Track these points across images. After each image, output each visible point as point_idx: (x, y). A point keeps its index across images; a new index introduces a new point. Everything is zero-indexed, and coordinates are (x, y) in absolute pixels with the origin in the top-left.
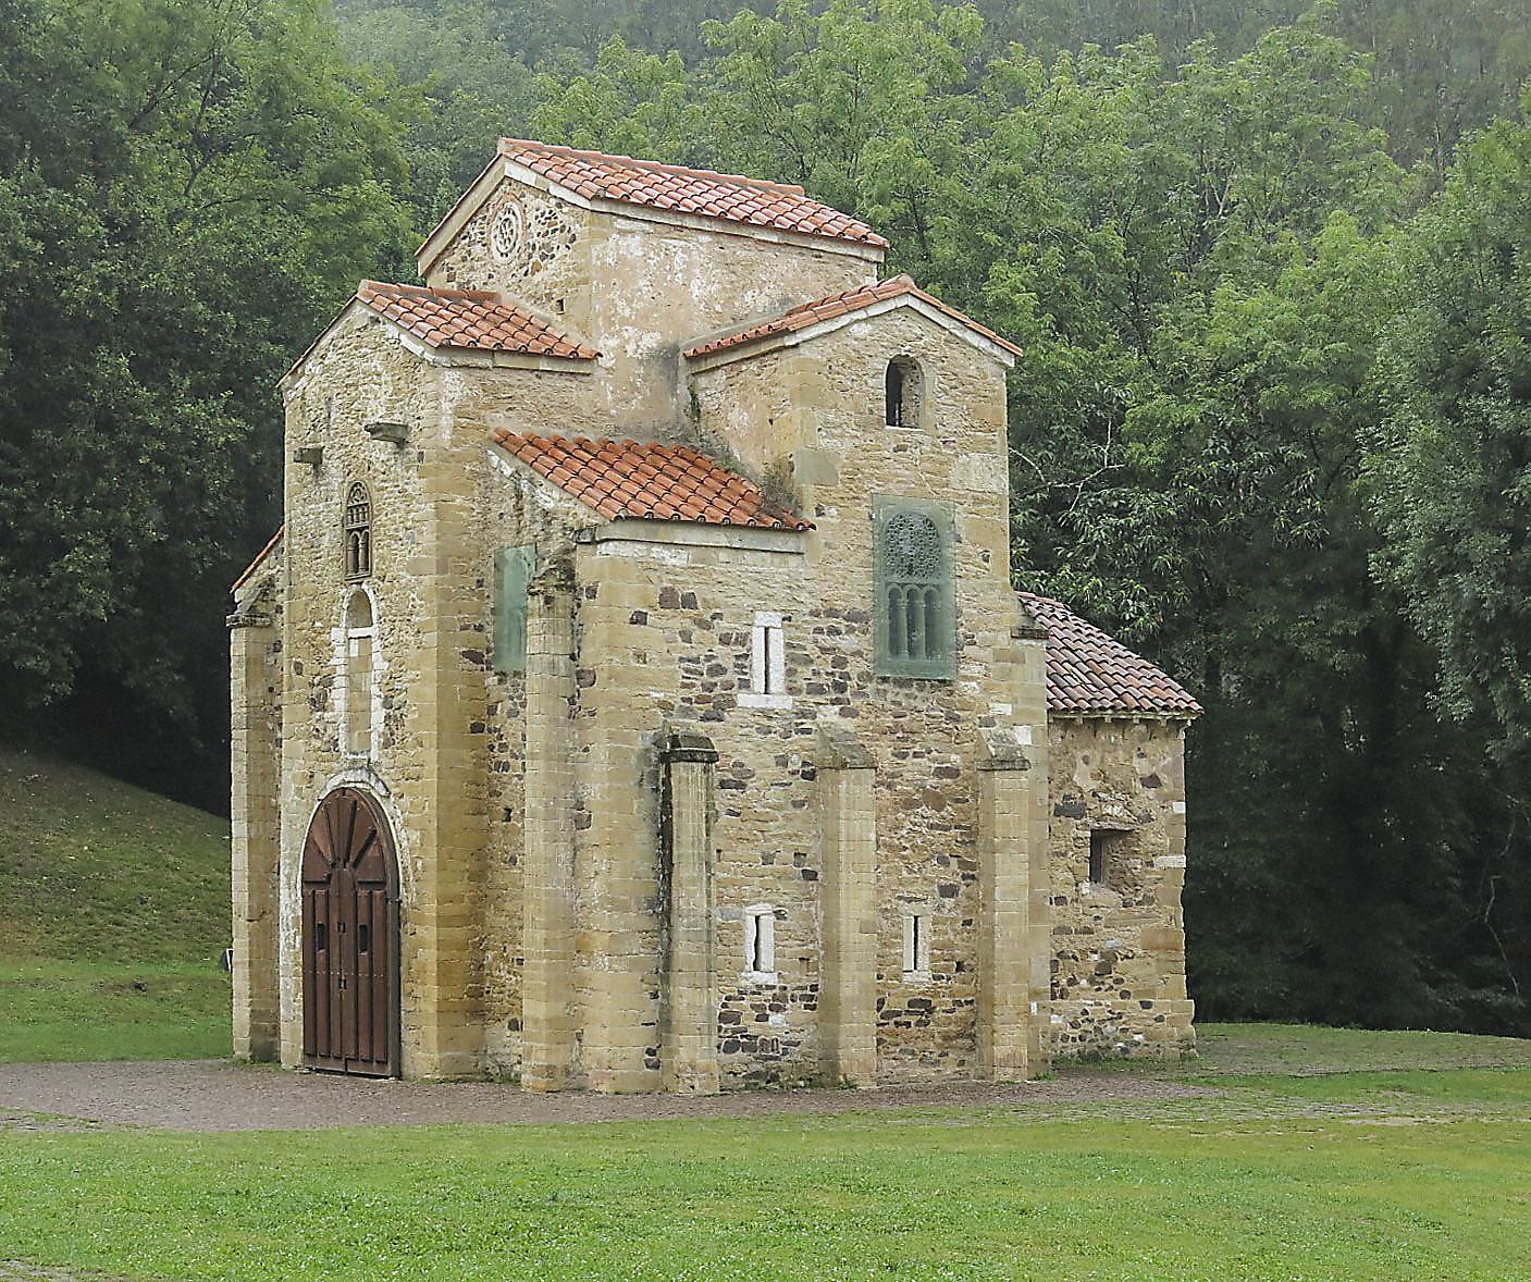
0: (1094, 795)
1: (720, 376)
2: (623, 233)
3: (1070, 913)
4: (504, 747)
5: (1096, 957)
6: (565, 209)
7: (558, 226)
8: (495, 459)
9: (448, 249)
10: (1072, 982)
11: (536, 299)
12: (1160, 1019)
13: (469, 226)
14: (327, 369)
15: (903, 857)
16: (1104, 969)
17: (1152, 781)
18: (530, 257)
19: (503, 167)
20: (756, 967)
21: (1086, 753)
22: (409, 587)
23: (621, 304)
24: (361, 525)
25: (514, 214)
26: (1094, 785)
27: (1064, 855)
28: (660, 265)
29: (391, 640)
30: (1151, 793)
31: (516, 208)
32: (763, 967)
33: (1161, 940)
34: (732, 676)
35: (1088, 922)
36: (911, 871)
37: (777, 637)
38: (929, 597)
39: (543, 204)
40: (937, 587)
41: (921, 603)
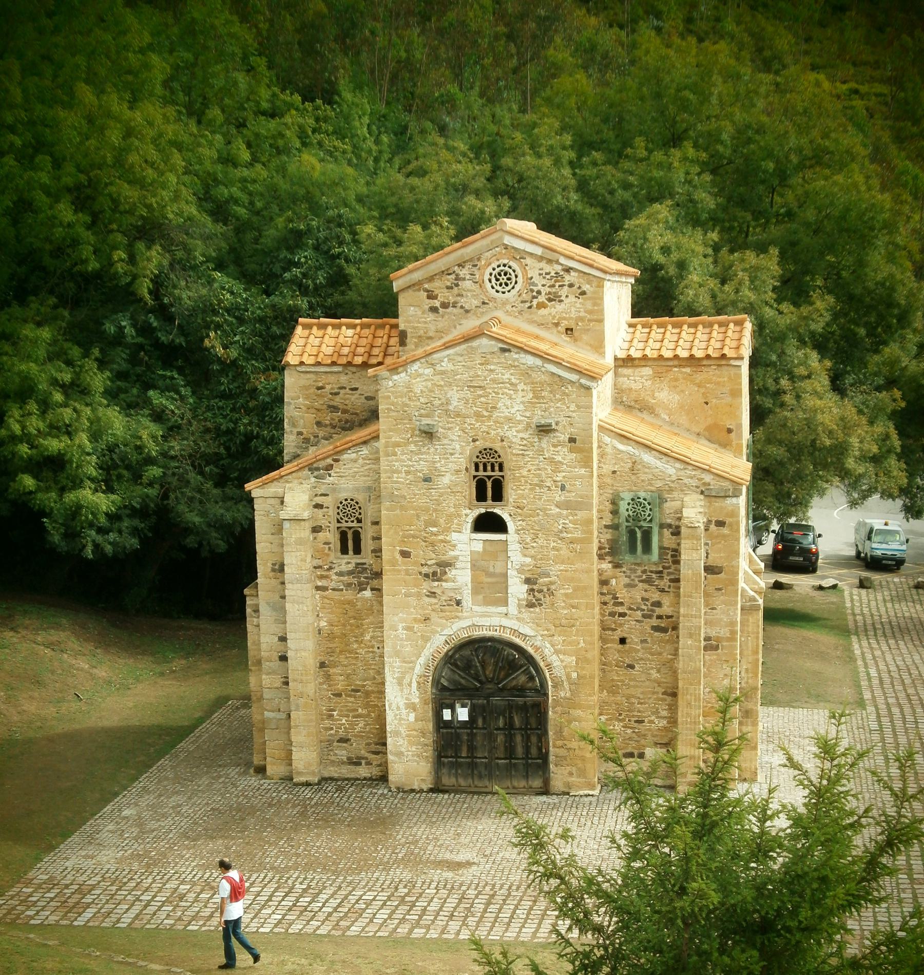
1: (648, 371)
4: (622, 604)
6: (573, 273)
7: (567, 283)
8: (607, 439)
9: (431, 279)
11: (540, 325)
14: (443, 373)
18: (534, 297)
19: (501, 238)
22: (559, 515)
24: (489, 473)
25: (510, 267)
29: (534, 545)
31: (511, 263)
39: (547, 268)
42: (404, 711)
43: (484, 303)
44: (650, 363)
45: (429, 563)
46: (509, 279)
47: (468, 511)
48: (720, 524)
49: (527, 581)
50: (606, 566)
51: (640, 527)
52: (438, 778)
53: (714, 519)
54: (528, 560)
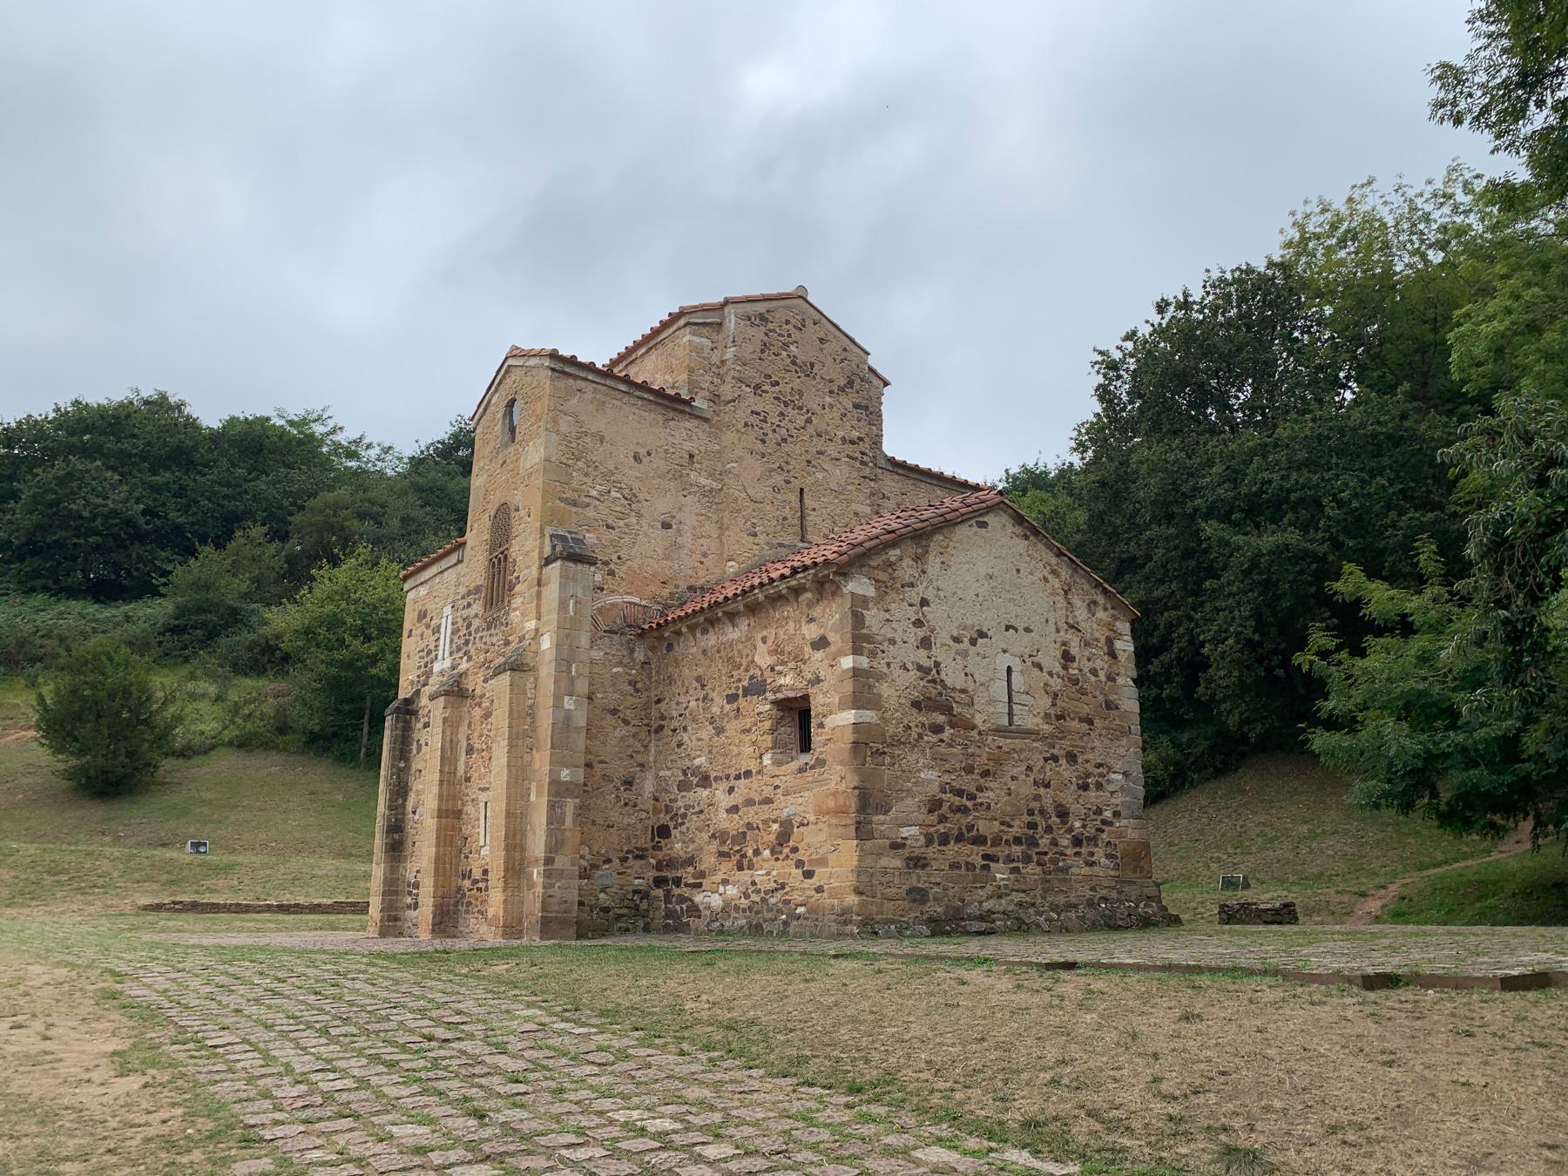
0: (773, 669)
3: (755, 786)
5: (776, 826)
10: (757, 852)
12: (819, 890)
16: (784, 836)
17: (821, 643)
21: (765, 633)
26: (770, 660)
27: (749, 731)
30: (819, 655)
33: (831, 804)
34: (433, 655)
35: (768, 791)
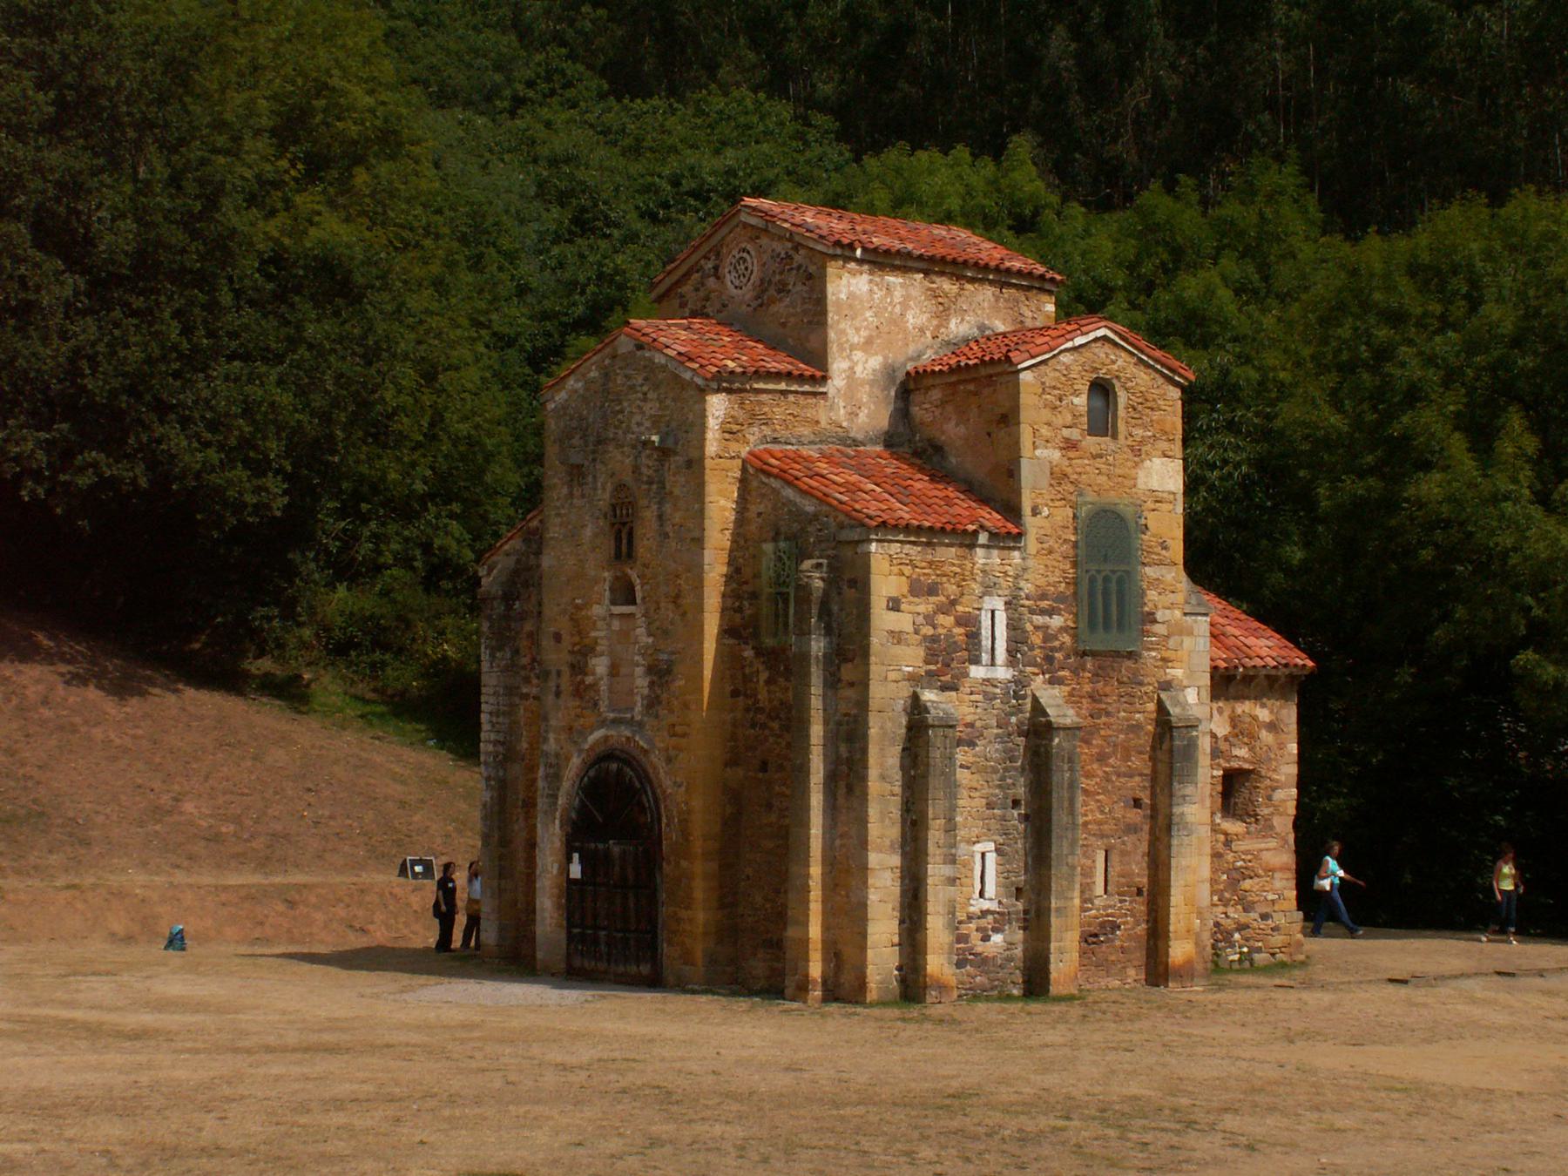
1: (936, 395)
2: (853, 273)
4: (760, 710)
6: (802, 252)
7: (795, 265)
13: (702, 262)
15: (1098, 801)
17: (1272, 727)
20: (982, 894)
23: (851, 332)
28: (882, 299)
31: (749, 247)
32: (987, 895)
36: (1102, 812)
37: (1001, 618)
38: (1120, 581)
40: (1128, 572)
41: (1113, 586)
42: (550, 859)
43: (724, 306)
44: (938, 381)
45: (576, 648)
46: (746, 269)
47: (606, 574)
48: (853, 583)
49: (650, 670)
50: (748, 653)
51: (781, 594)
52: (569, 955)
53: (847, 576)
54: (650, 640)
